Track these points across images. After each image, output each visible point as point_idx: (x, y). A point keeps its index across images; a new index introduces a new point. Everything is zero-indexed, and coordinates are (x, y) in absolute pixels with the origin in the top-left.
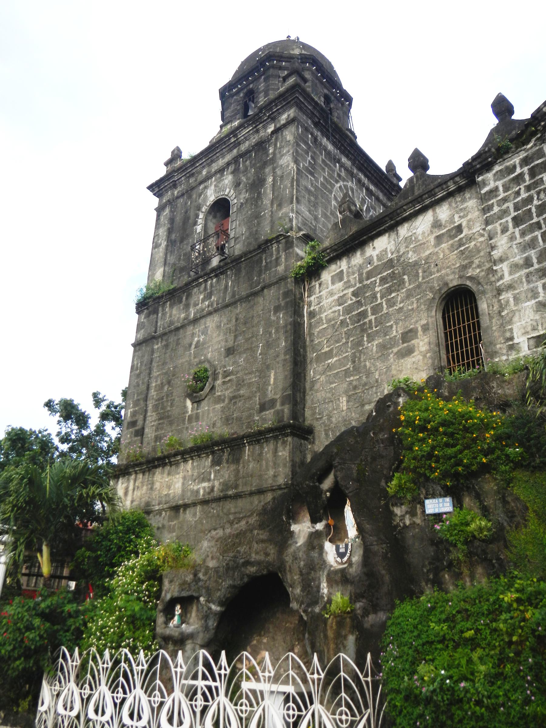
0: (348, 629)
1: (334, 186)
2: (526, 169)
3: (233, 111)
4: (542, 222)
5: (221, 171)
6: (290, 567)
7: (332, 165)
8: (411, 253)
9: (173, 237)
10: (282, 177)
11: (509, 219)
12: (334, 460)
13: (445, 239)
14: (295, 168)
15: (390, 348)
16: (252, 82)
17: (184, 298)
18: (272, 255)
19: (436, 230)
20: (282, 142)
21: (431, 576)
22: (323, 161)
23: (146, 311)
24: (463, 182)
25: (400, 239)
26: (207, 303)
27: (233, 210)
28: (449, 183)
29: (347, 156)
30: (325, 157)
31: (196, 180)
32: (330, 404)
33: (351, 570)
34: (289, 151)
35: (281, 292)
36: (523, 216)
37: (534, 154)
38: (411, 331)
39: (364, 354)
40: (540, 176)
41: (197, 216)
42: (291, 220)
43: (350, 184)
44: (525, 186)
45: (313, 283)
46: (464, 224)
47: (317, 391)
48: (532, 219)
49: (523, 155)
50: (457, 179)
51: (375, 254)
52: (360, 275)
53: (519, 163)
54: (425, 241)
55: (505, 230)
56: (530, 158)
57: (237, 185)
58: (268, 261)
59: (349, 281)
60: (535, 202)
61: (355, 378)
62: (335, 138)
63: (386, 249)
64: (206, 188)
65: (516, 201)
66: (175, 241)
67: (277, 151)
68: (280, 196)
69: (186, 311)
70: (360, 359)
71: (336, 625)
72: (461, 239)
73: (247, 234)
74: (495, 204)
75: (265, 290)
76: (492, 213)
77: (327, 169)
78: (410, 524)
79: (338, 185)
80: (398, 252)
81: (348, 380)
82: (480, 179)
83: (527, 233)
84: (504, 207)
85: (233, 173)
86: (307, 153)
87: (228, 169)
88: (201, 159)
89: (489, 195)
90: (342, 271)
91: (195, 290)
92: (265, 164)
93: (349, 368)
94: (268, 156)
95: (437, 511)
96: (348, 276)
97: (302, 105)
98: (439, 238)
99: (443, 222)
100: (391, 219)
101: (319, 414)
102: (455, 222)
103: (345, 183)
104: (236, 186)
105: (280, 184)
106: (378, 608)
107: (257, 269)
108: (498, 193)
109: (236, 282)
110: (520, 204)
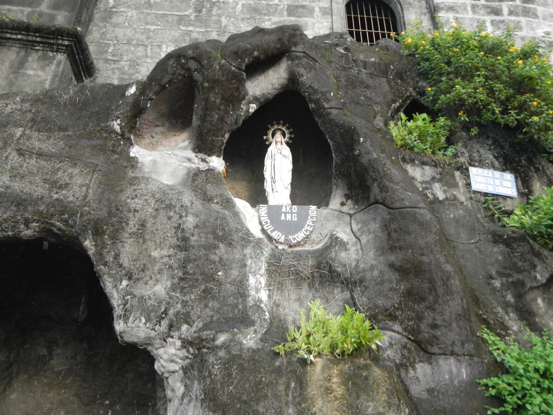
0: (385, 397)
6: (143, 225)
12: (295, 44)
15: (265, 14)
21: (510, 298)
32: (141, 49)
33: (343, 255)
38: (303, 7)
39: (219, 8)
47: (116, 25)
61: (198, 29)
70: (210, 11)
71: (344, 383)
78: (447, 199)
81: (182, 28)
93: (188, 16)
95: (490, 189)
101: (113, 55)
106: (435, 350)
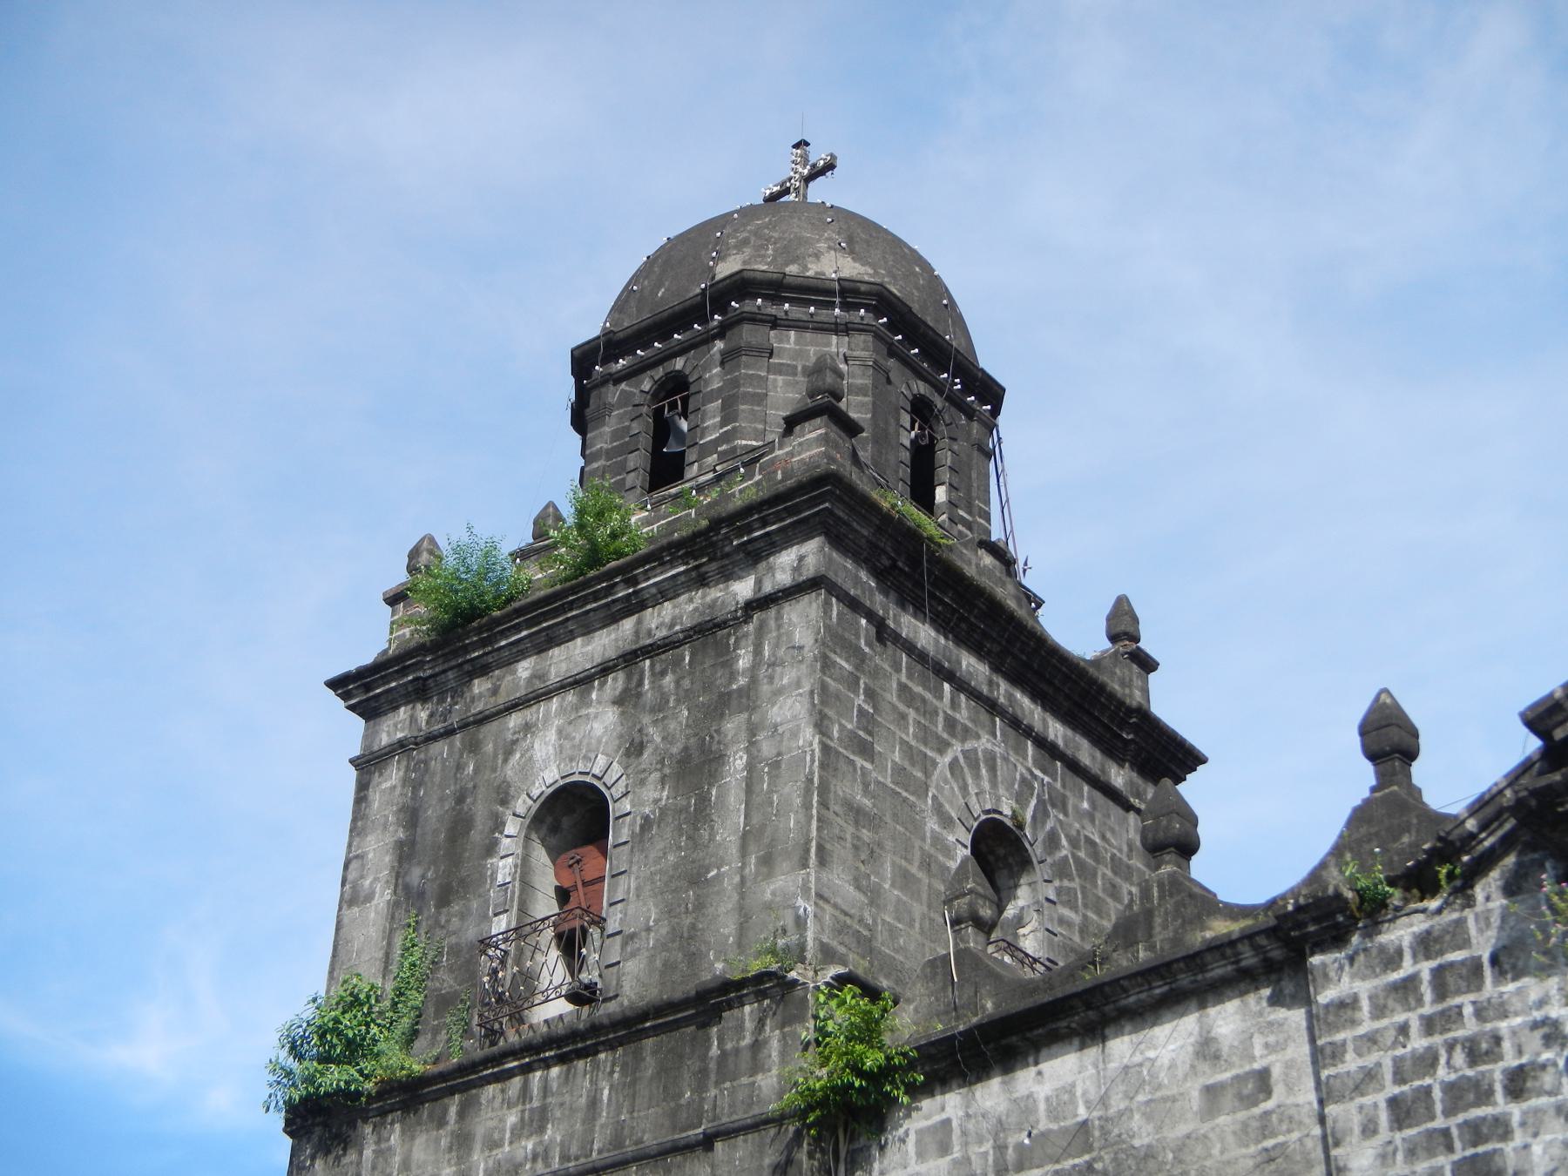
1: (934, 764)
2: (1426, 968)
3: (616, 435)
4: (1455, 1132)
5: (581, 682)
7: (928, 696)
8: (1137, 1121)
9: (415, 875)
10: (775, 765)
11: (1378, 1099)
13: (1228, 1100)
14: (816, 746)
16: (683, 350)
17: (453, 1111)
18: (740, 1028)
19: (1204, 1067)
20: (777, 646)
22: (903, 688)
23: (318, 1131)
24: (1277, 954)
25: (1112, 1065)
26: (530, 1146)
27: (619, 833)
28: (1240, 947)
29: (978, 651)
30: (910, 676)
31: (495, 691)
34: (798, 685)
35: (767, 1161)
36: (1413, 1102)
37: (1445, 931)
40: (1457, 1000)
41: (499, 825)
42: (800, 923)
43: (984, 743)
44: (1422, 1017)
45: (862, 1141)
46: (1276, 1072)
48: (1432, 1118)
49: (1419, 924)
50: (1262, 941)
51: (1043, 1091)
52: (1000, 1148)
53: (1411, 947)
54: (1174, 1091)
55: (1369, 1130)
56: (1436, 940)
57: (634, 749)
58: (729, 1046)
59: (967, 1160)
60: (1442, 1072)
62: (941, 602)
63: (1073, 1085)
64: (528, 728)
65: (1400, 1052)
66: (421, 895)
67: (762, 672)
68: (769, 831)
69: (460, 1160)
72: (1267, 1114)
73: (664, 931)
74: (1350, 1047)
75: (719, 1146)
76: (1341, 1069)
77: (912, 714)
79: (947, 759)
80: (1104, 1101)
82: (1316, 960)
83: (1420, 1152)
84: (1370, 1060)
85: (619, 701)
86: (853, 683)
87: (602, 685)
88: (517, 628)
89: (1337, 1015)
90: (947, 1122)
91: (491, 1090)
92: (722, 704)
94: (733, 676)
96: (966, 1144)
97: (843, 530)
98: (1211, 1092)
99: (1225, 1050)
100: (1089, 1007)
102: (1253, 1058)
103: (968, 745)
104: (628, 754)
105: (770, 791)
107: (693, 1064)
108: (1358, 1015)
109: (629, 1088)
110: (1408, 1063)
